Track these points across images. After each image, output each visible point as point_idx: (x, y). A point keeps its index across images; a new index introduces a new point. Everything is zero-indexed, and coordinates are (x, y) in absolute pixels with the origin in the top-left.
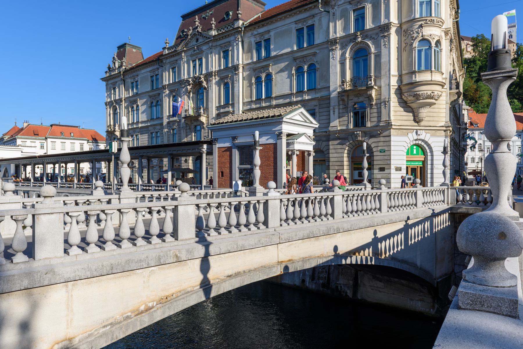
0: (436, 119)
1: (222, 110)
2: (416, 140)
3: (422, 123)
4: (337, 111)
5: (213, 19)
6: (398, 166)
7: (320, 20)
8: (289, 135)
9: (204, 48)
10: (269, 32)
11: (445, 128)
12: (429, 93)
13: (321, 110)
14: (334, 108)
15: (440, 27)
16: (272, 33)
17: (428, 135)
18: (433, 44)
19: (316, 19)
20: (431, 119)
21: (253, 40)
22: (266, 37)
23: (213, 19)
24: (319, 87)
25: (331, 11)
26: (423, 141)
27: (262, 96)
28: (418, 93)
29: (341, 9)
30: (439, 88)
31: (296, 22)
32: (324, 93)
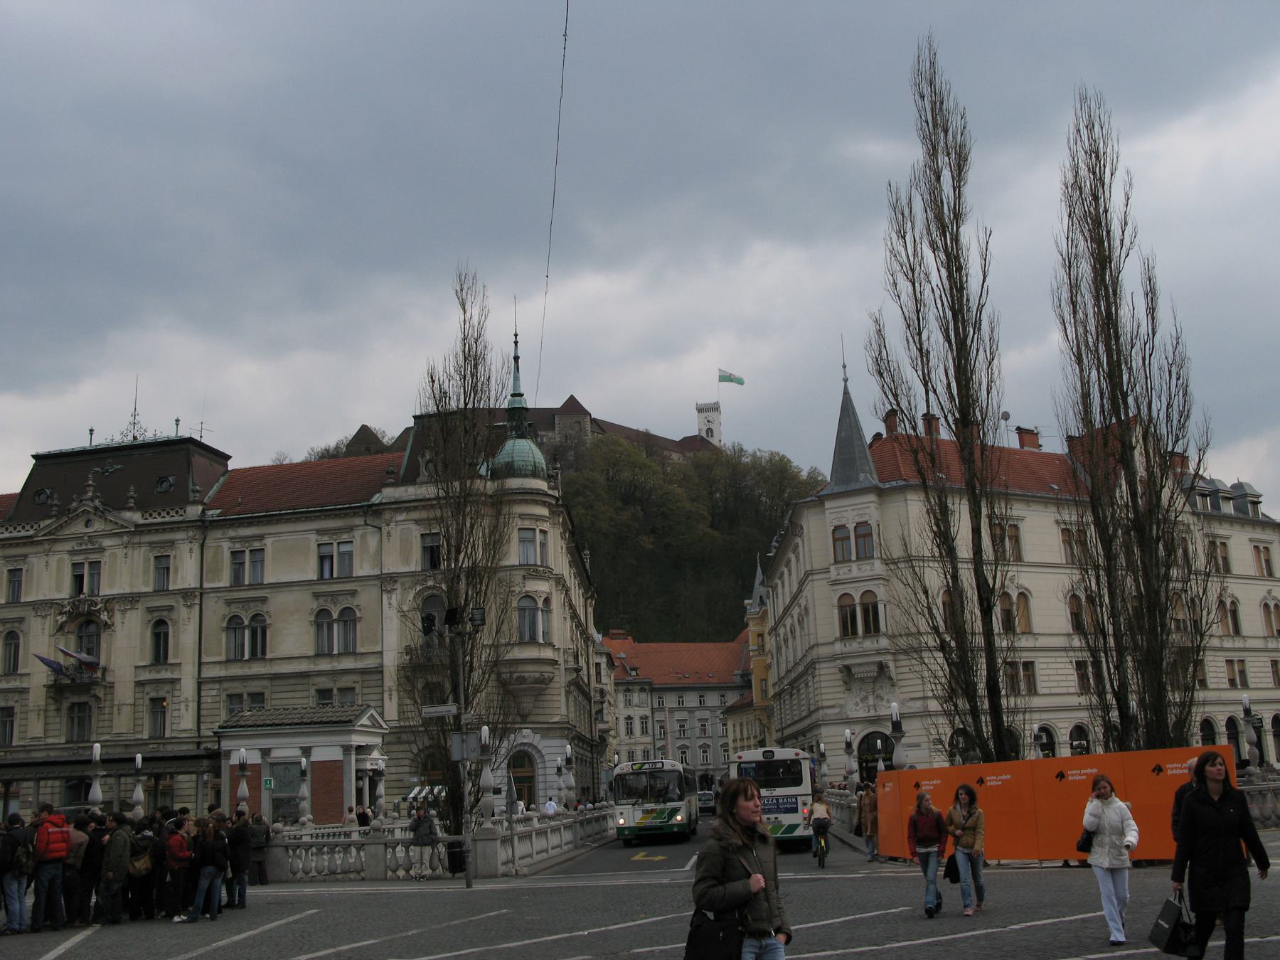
0: (547, 711)
1: (146, 676)
3: (529, 719)
4: (395, 694)
5: (132, 488)
7: (363, 537)
8: (359, 748)
9: (107, 542)
10: (261, 537)
12: (537, 675)
13: (366, 691)
14: (390, 690)
15: (547, 579)
16: (269, 541)
17: (538, 736)
18: (540, 604)
19: (357, 534)
20: (541, 711)
21: (226, 546)
22: (257, 545)
23: (132, 488)
24: (362, 650)
25: (385, 529)
27: (243, 655)
29: (400, 528)
30: (549, 669)
31: (319, 532)
32: (370, 662)
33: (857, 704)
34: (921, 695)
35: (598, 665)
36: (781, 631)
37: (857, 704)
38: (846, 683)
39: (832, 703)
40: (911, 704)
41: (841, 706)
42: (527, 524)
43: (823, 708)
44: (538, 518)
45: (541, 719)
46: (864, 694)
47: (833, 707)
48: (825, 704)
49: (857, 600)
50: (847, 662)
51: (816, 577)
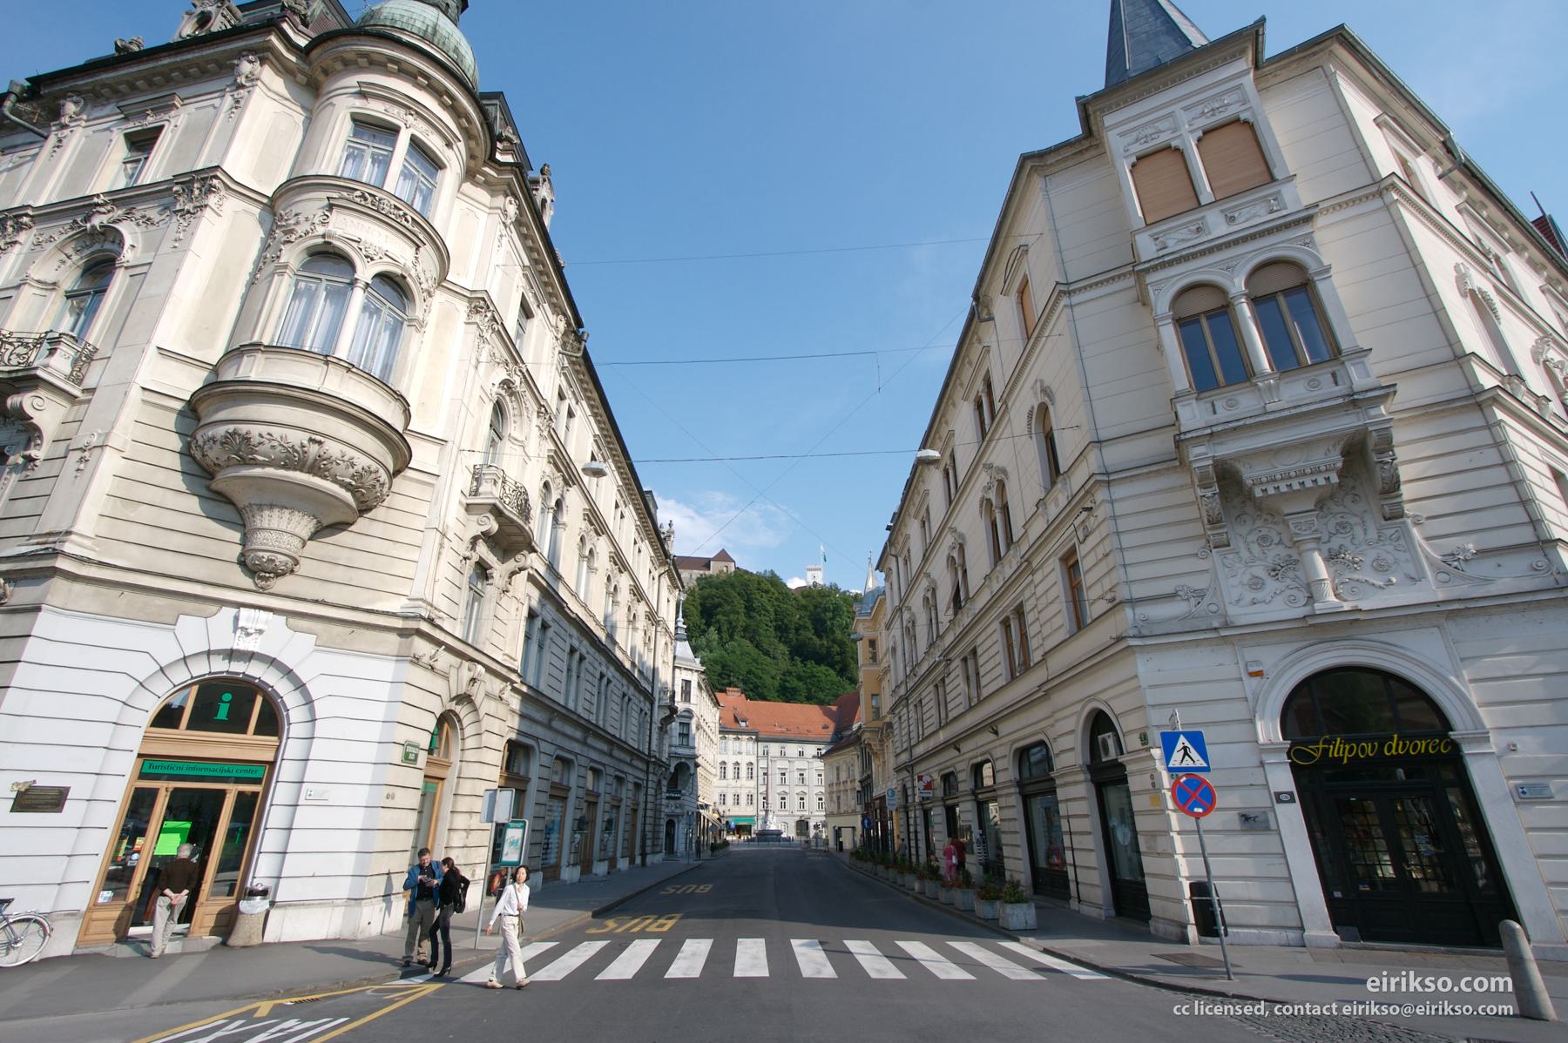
2: (231, 654)
6: (44, 781)
11: (399, 624)
12: (296, 438)
26: (272, 662)
28: (243, 428)
33: (1256, 584)
34: (1526, 535)
35: (688, 683)
36: (916, 602)
37: (1256, 584)
38: (1214, 522)
39: (1167, 587)
40: (1486, 567)
41: (1200, 594)
42: (376, 109)
43: (1133, 602)
44: (410, 106)
45: (332, 594)
46: (1276, 553)
47: (1172, 596)
48: (1138, 591)
49: (1237, 285)
50: (1226, 449)
51: (1076, 299)
